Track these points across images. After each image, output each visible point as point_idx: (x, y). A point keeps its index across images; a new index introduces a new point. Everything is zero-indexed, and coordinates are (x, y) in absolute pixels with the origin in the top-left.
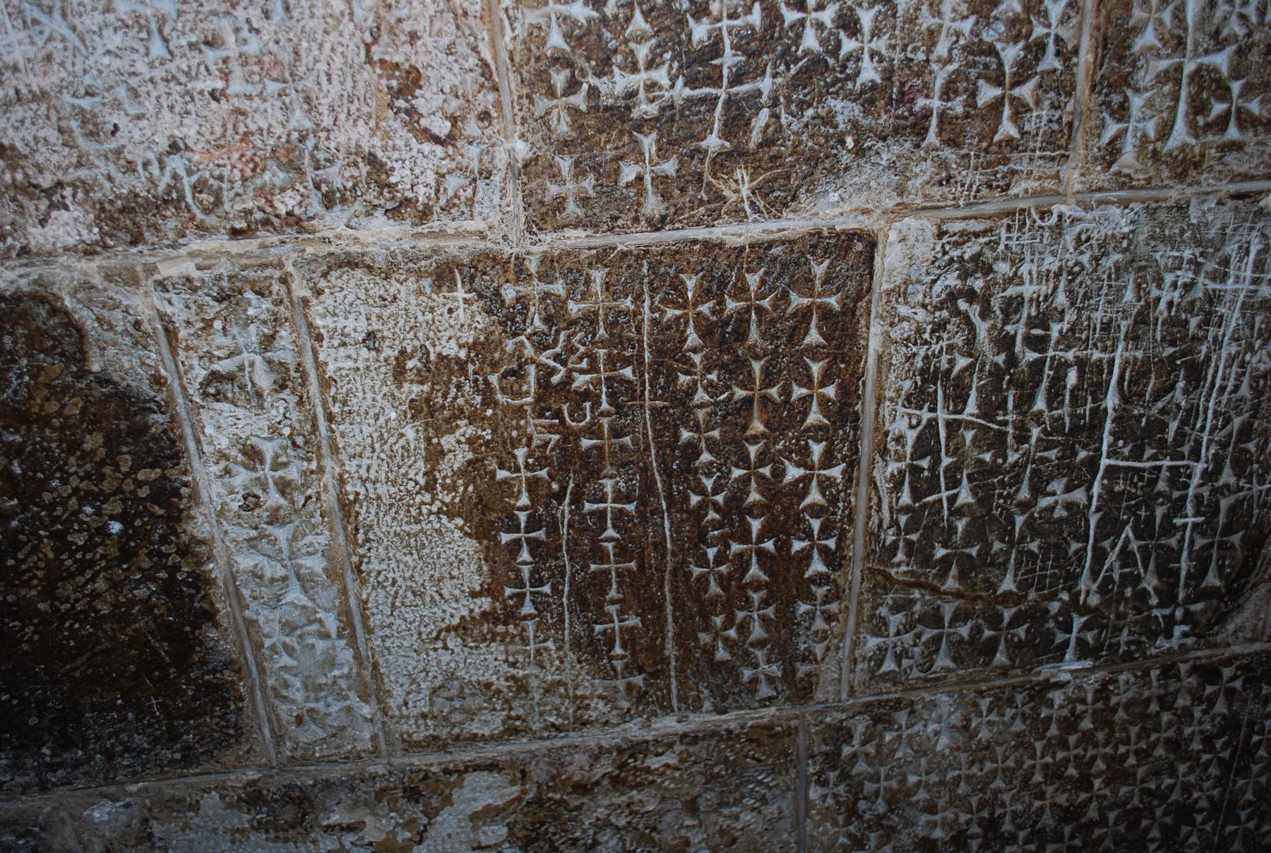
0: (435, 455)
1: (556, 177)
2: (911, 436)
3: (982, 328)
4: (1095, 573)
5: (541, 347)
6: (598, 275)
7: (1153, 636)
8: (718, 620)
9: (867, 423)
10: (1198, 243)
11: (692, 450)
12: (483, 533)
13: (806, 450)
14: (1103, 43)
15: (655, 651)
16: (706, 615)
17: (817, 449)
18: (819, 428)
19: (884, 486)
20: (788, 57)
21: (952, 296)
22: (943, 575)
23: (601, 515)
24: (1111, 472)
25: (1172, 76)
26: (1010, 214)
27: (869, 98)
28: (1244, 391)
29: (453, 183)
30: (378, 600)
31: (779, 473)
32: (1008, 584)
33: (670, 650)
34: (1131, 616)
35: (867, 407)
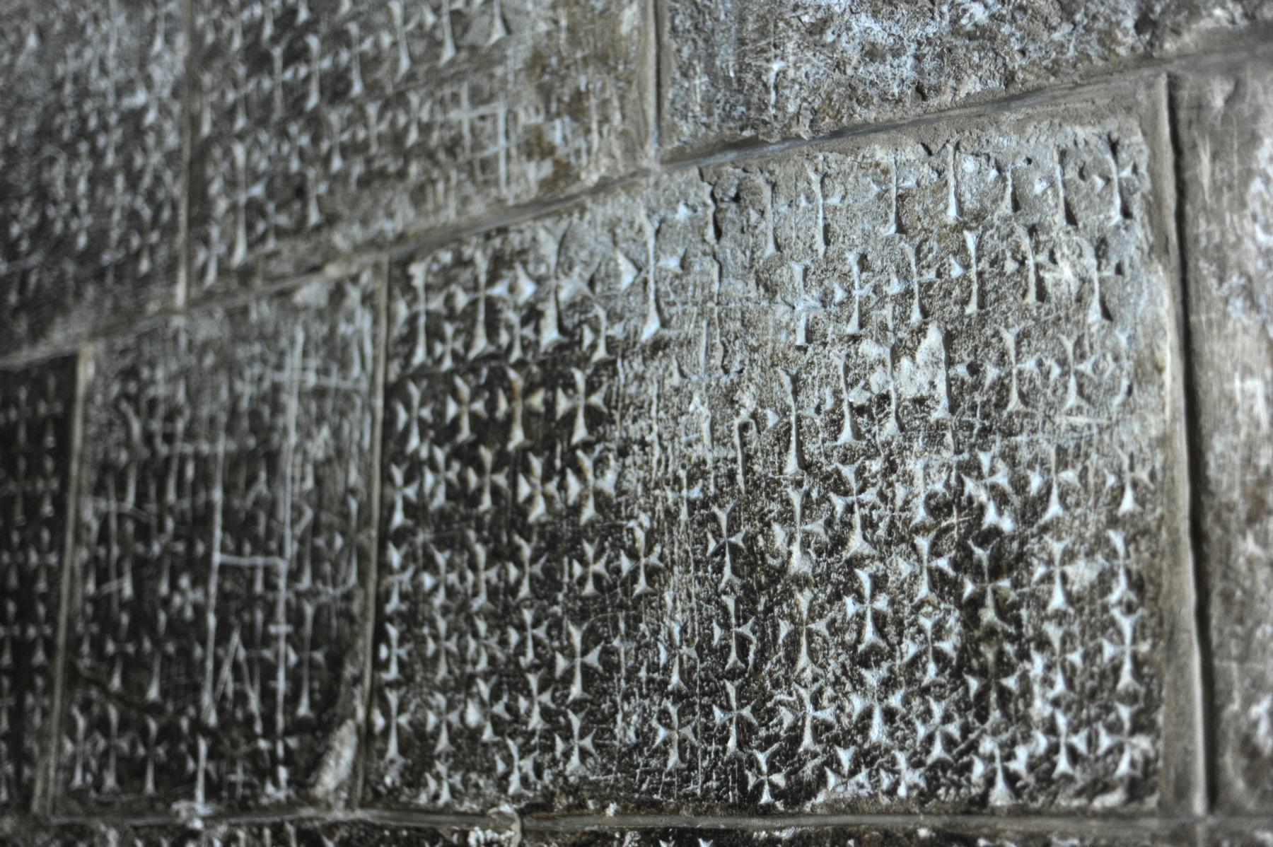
3: (136, 427)
32: (153, 693)
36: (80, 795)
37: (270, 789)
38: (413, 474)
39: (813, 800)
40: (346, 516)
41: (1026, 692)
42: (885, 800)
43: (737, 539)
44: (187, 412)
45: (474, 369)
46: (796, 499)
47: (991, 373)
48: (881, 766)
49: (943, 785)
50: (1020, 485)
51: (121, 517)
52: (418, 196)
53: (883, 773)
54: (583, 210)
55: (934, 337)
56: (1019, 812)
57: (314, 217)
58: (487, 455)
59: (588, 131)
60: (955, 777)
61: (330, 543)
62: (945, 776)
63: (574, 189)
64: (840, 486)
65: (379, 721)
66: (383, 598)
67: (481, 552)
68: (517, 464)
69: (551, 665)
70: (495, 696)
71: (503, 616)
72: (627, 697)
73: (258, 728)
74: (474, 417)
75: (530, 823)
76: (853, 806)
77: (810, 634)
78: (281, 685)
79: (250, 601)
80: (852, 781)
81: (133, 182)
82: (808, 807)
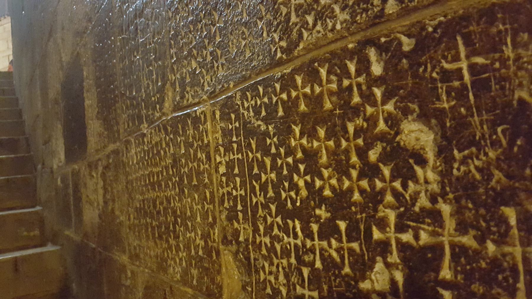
39: (298, 48)
42: (330, 35)
48: (327, 16)
49: (359, 13)
53: (328, 20)
60: (365, 6)
62: (359, 8)
76: (317, 46)
80: (314, 31)
82: (296, 53)
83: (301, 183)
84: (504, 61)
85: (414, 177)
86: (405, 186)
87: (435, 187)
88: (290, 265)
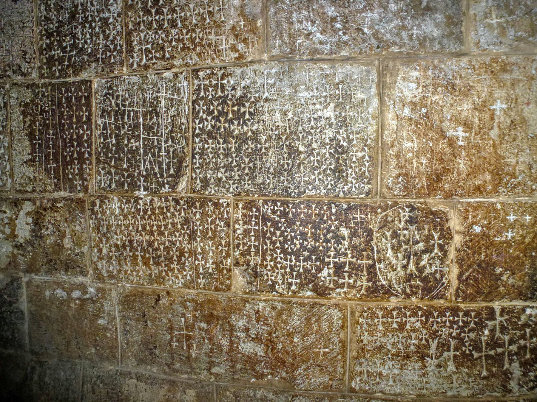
0: (25, 122)
1: (43, 69)
2: (102, 125)
3: (113, 101)
4: (144, 166)
5: (41, 101)
6: (50, 88)
7: (161, 187)
8: (69, 167)
9: (93, 121)
10: (152, 84)
11: (63, 125)
12: (31, 140)
13: (83, 127)
14: (127, 44)
15: (58, 173)
16: (67, 165)
17: (85, 127)
18: (85, 122)
19: (98, 137)
20: (76, 48)
21: (106, 94)
22: (111, 161)
23: (49, 138)
24: (144, 138)
25: (141, 50)
26: (115, 77)
27: (89, 55)
28: (170, 120)
29: (30, 70)
30: (14, 153)
31: (79, 132)
32: (125, 166)
33: (61, 174)
34: (154, 180)
35: (93, 118)
36: (103, 189)
37: (163, 189)
38: (202, 120)
40: (181, 130)
41: (347, 176)
43: (288, 143)
44: (129, 100)
45: (218, 99)
46: (301, 136)
47: (343, 114)
50: (348, 137)
51: (110, 124)
52: (199, 55)
54: (247, 66)
55: (332, 105)
56: (346, 198)
57: (167, 55)
58: (222, 119)
59: (248, 48)
61: (177, 135)
63: (244, 61)
64: (310, 134)
65: (194, 176)
66: (193, 150)
67: (221, 141)
68: (231, 122)
69: (240, 166)
70: (226, 172)
71: (227, 154)
72: (259, 173)
73: (159, 176)
74: (218, 110)
75: (235, 198)
76: (312, 196)
77: (304, 163)
78: (165, 166)
79: (154, 147)
81: (106, 38)
83: (297, 242)
84: (368, 218)
85: (341, 244)
86: (338, 246)
87: (347, 246)
88: (286, 272)
